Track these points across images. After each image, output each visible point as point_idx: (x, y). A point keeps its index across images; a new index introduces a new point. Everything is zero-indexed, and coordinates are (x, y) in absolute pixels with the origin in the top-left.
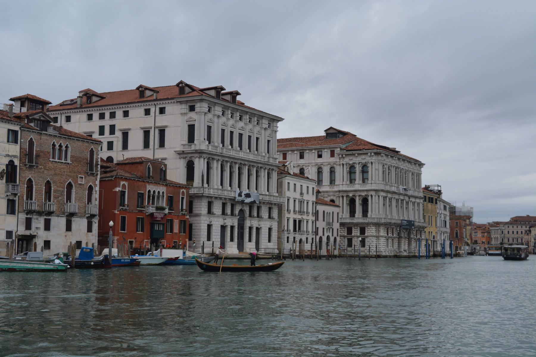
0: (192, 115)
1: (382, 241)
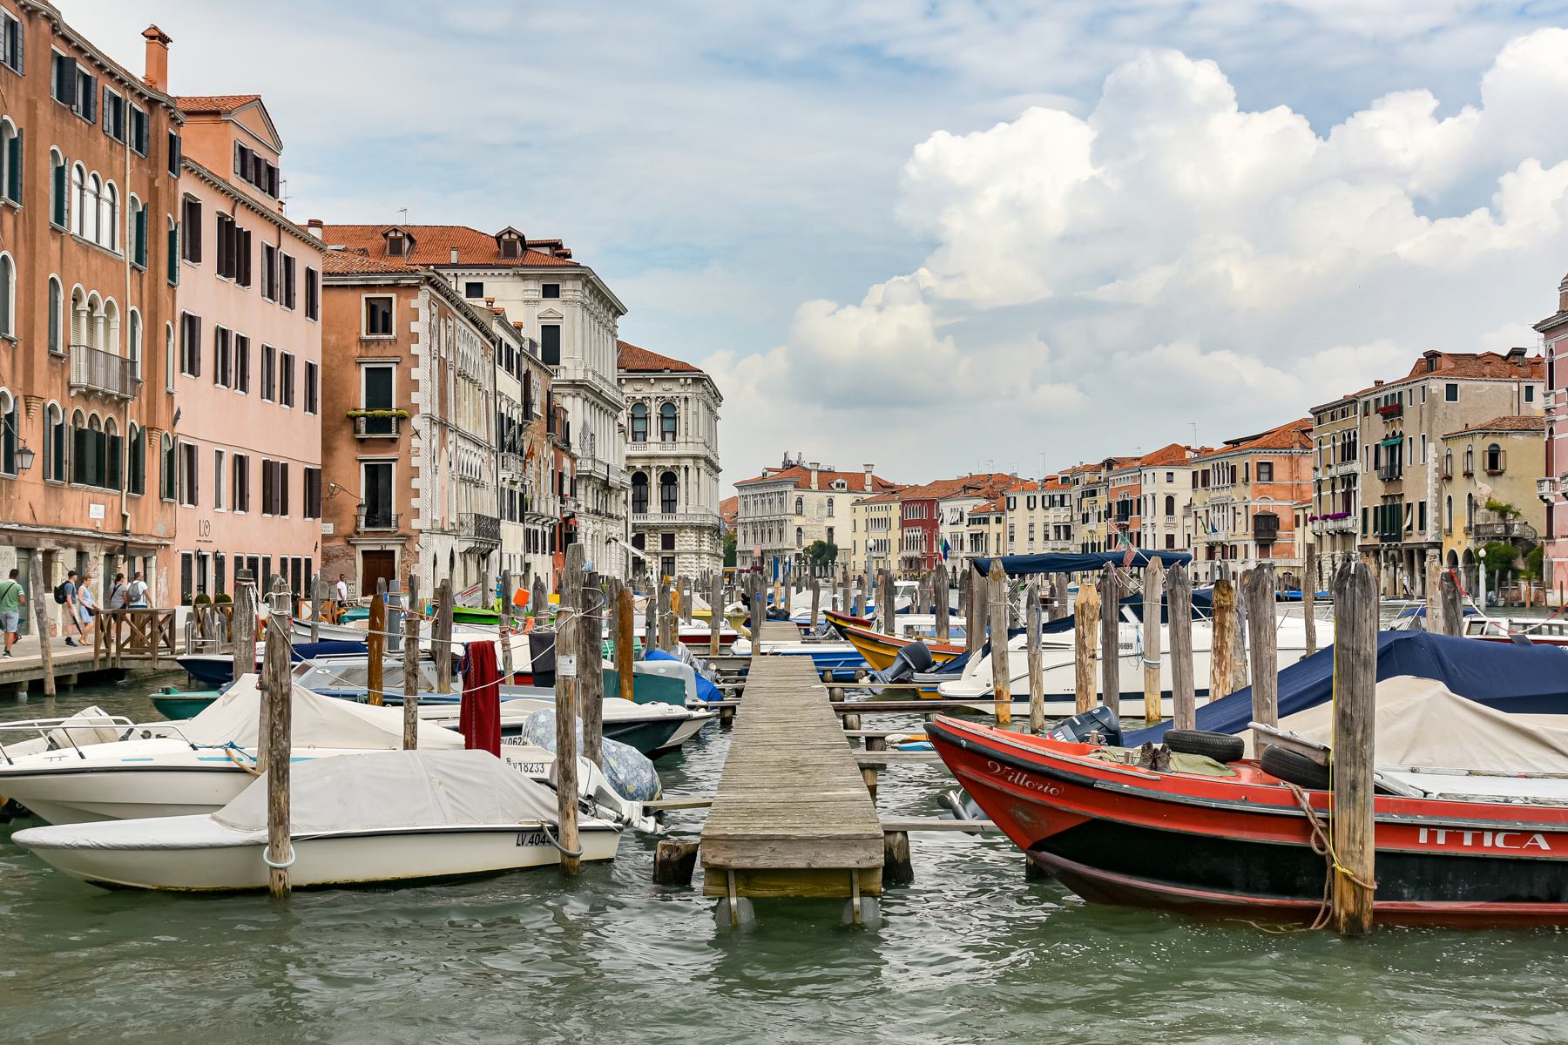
0: (551, 303)
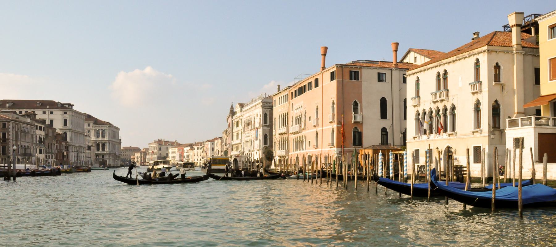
0: (66, 115)
1: (111, 160)
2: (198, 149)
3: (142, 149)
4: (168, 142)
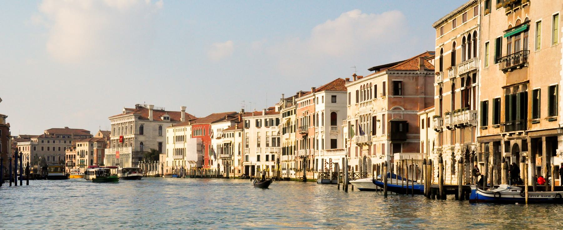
2: (258, 124)
3: (95, 133)
4: (163, 111)
